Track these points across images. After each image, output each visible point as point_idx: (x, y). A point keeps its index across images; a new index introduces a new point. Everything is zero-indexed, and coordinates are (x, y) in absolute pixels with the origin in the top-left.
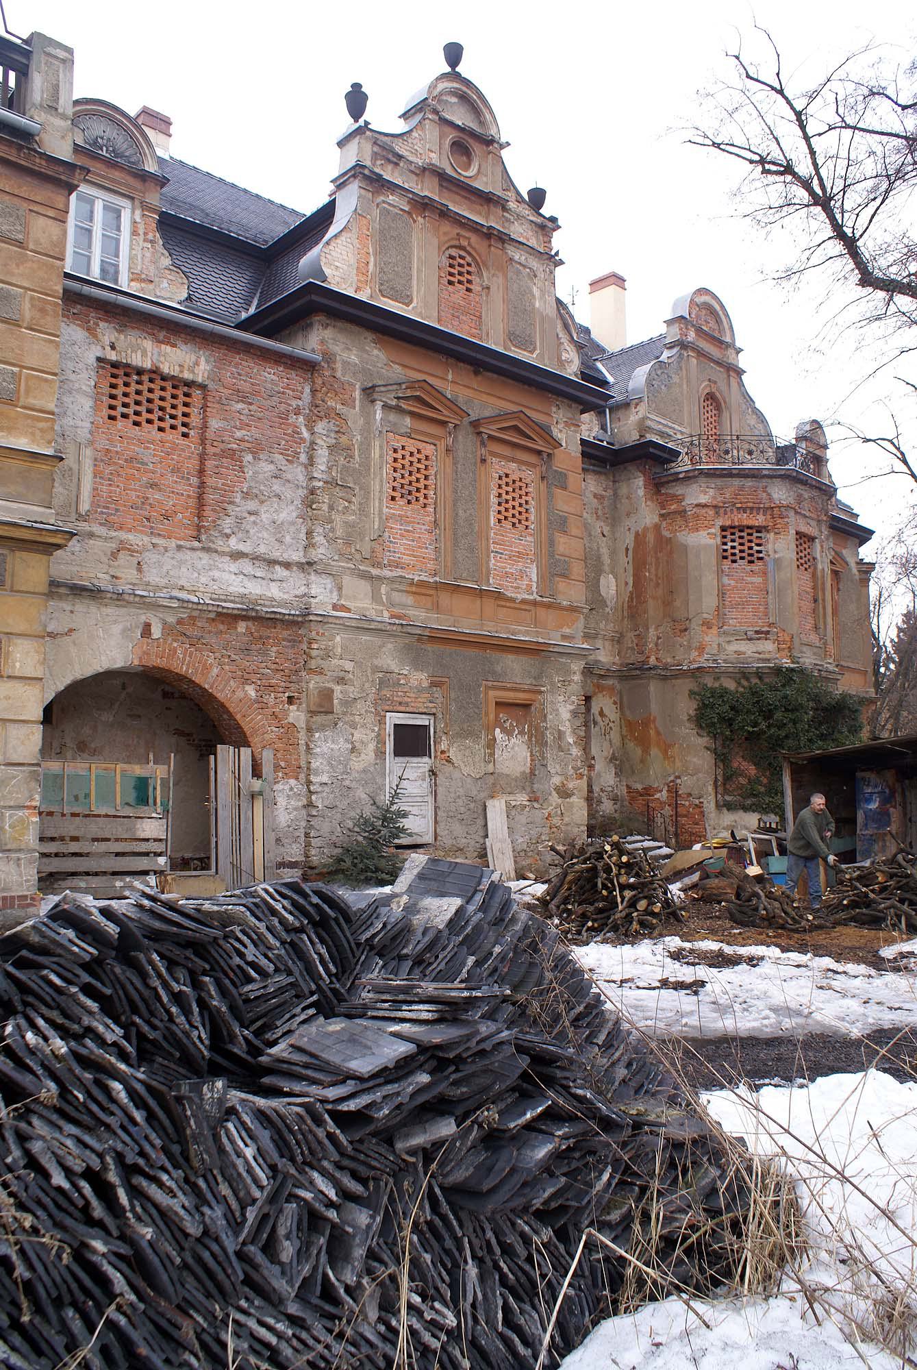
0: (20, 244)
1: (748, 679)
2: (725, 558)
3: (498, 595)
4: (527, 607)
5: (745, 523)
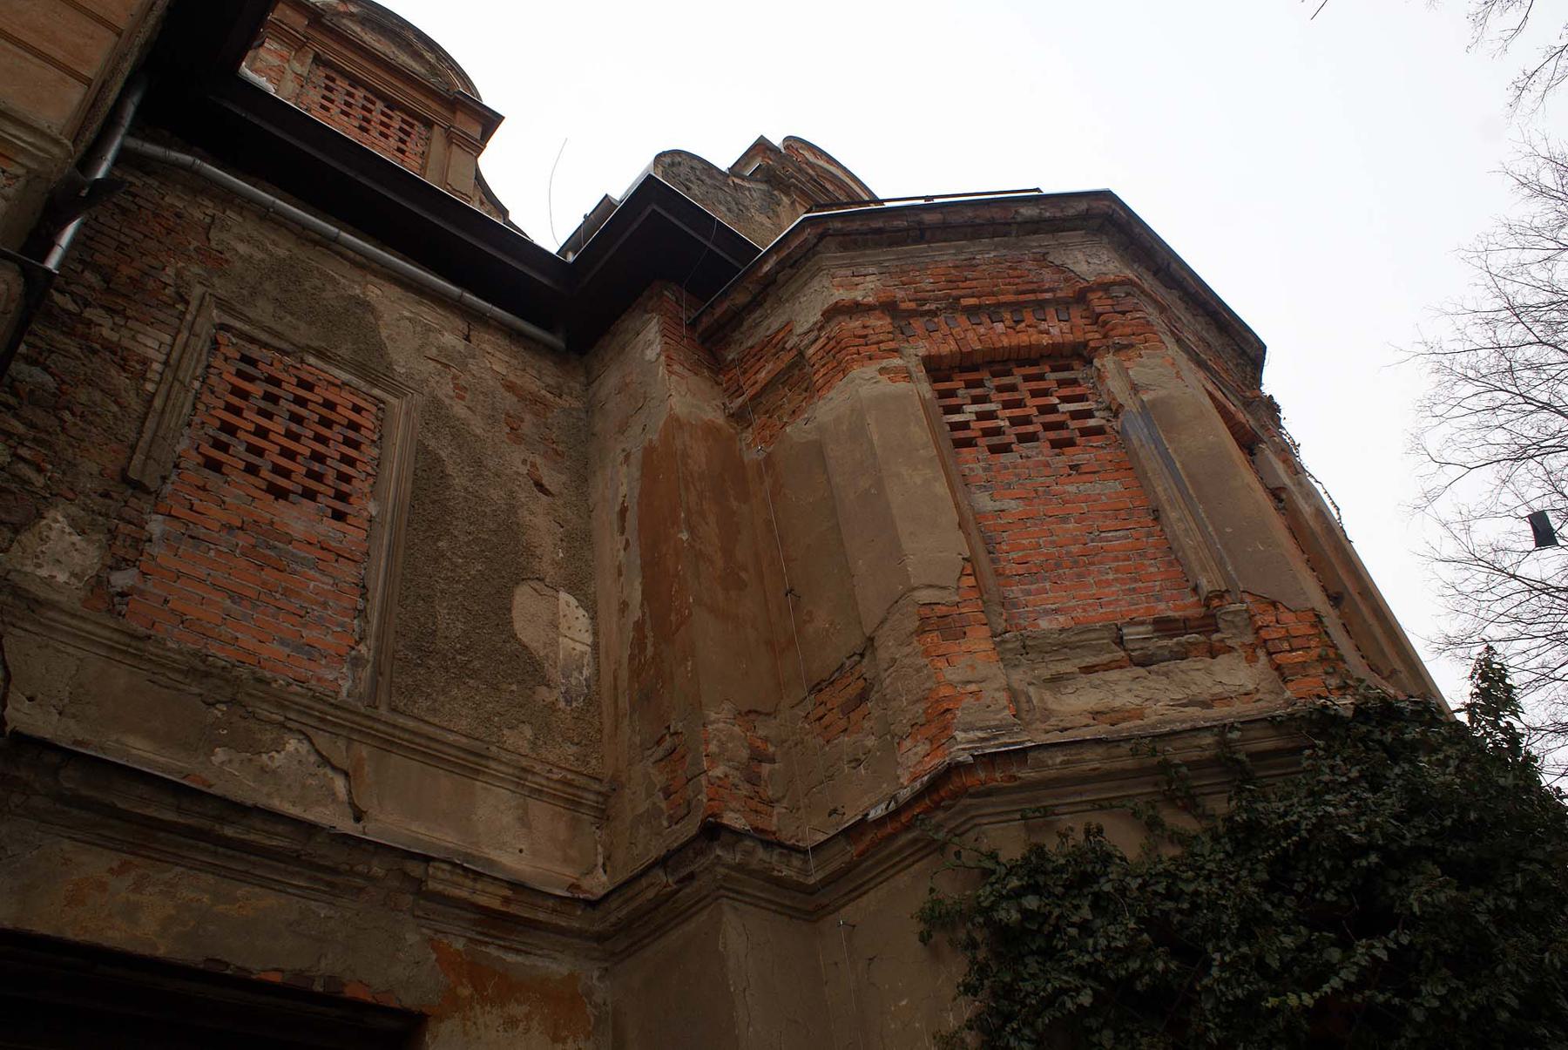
1: (1190, 803)
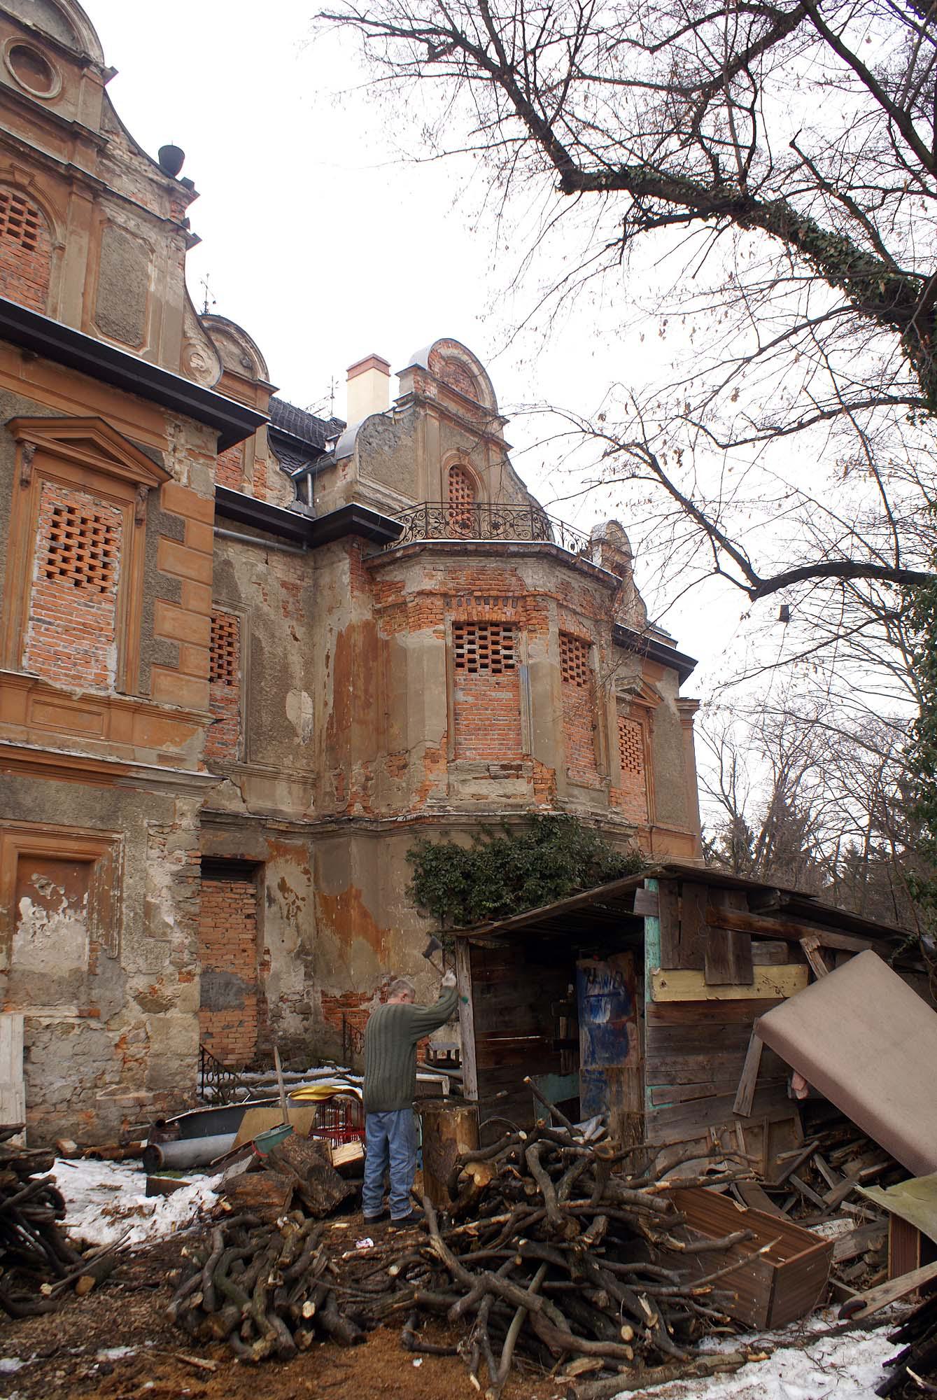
1: (490, 834)
2: (461, 665)
3: (34, 686)
4: (95, 708)
5: (487, 617)
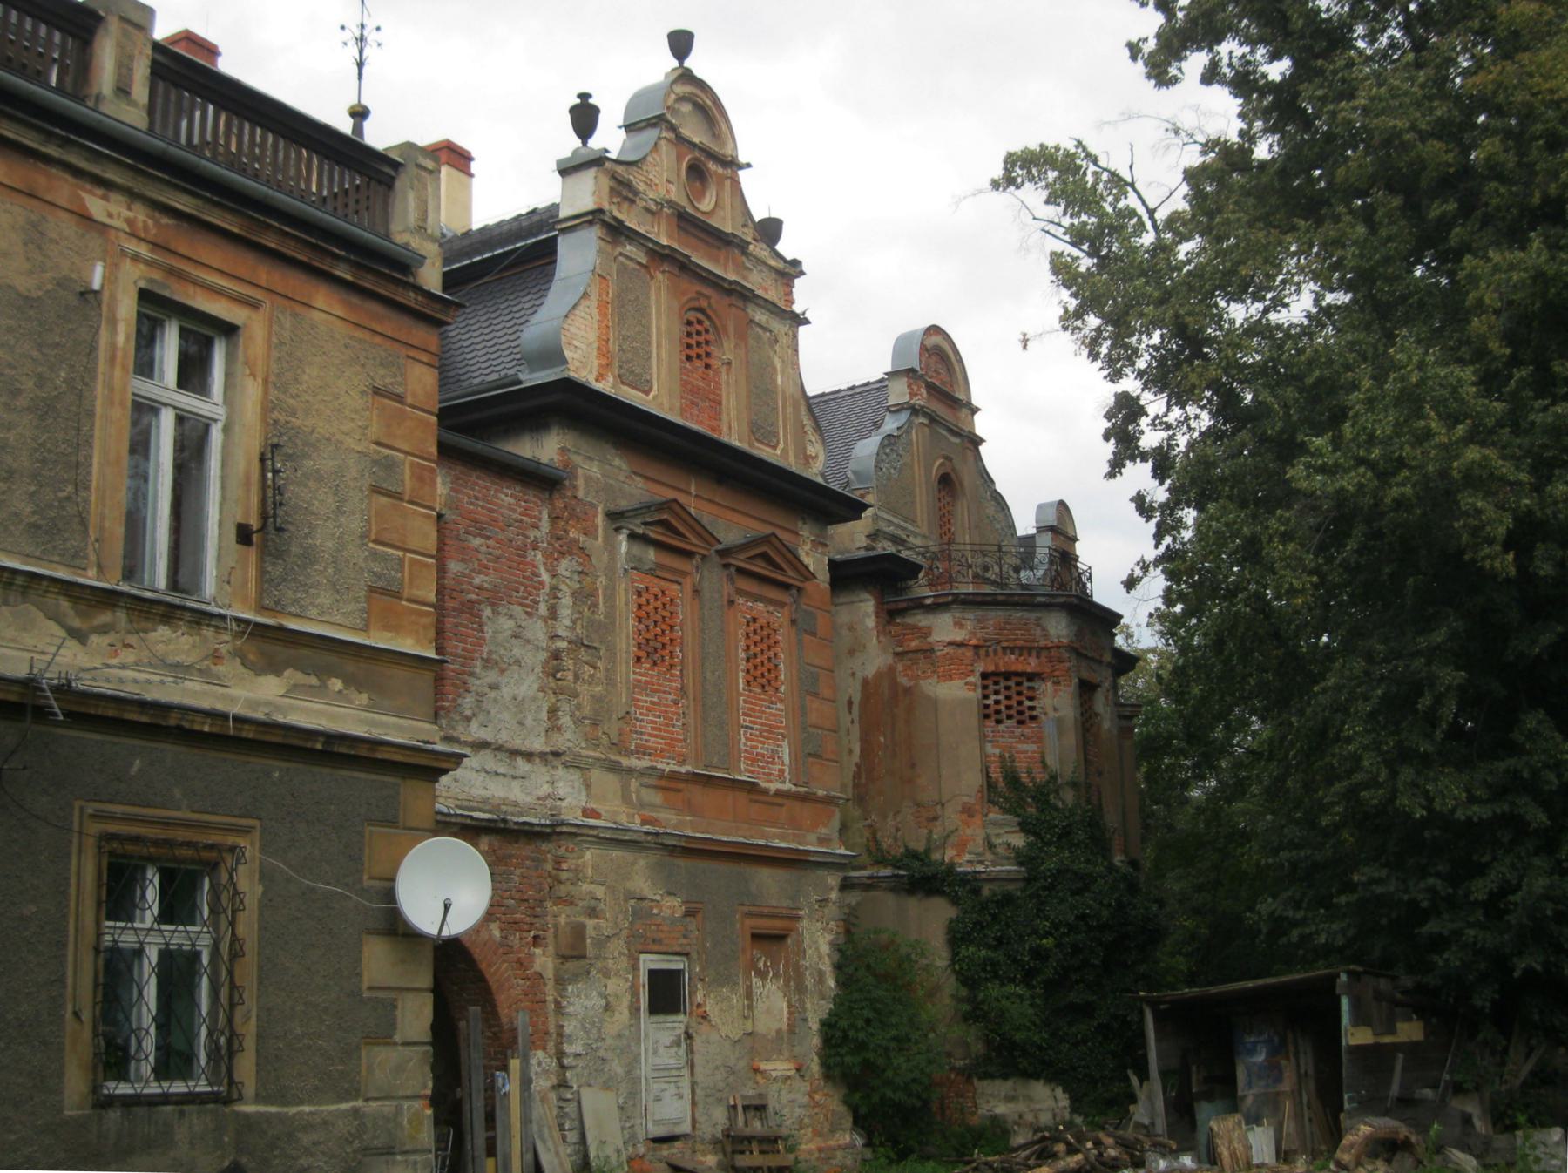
0: (400, 399)
2: (987, 716)
3: (751, 787)
5: (1013, 668)
